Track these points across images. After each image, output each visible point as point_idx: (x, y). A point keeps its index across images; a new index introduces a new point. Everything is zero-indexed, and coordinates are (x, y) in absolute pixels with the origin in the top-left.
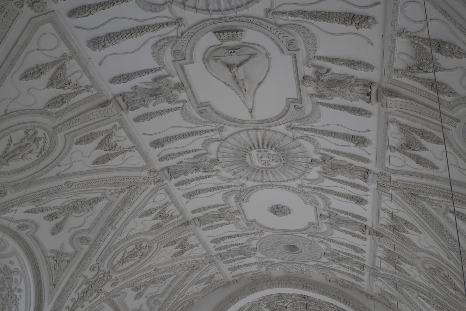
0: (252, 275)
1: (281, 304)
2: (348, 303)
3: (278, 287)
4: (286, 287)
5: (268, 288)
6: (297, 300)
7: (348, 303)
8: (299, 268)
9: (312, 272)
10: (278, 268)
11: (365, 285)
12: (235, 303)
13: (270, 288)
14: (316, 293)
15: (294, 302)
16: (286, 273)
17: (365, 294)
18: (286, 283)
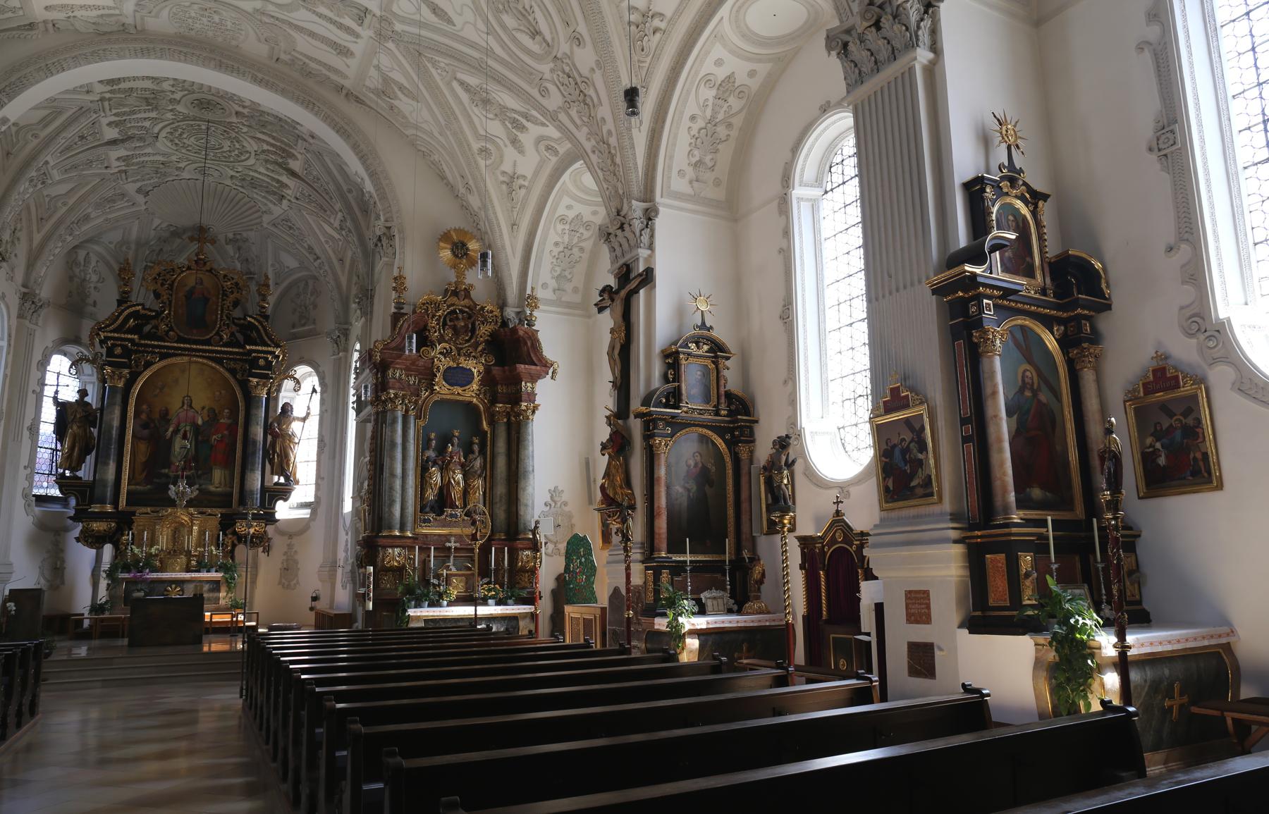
0: (98, 16)
1: (147, 124)
2: (311, 106)
3: (161, 58)
4: (180, 60)
5: (136, 57)
6: (186, 118)
7: (311, 106)
8: (216, 18)
9: (243, 33)
10: (167, 10)
11: (349, 69)
12: (52, 74)
13: (143, 56)
14: (245, 80)
15: (178, 122)
16: (182, 30)
17: (344, 92)
18: (181, 52)
